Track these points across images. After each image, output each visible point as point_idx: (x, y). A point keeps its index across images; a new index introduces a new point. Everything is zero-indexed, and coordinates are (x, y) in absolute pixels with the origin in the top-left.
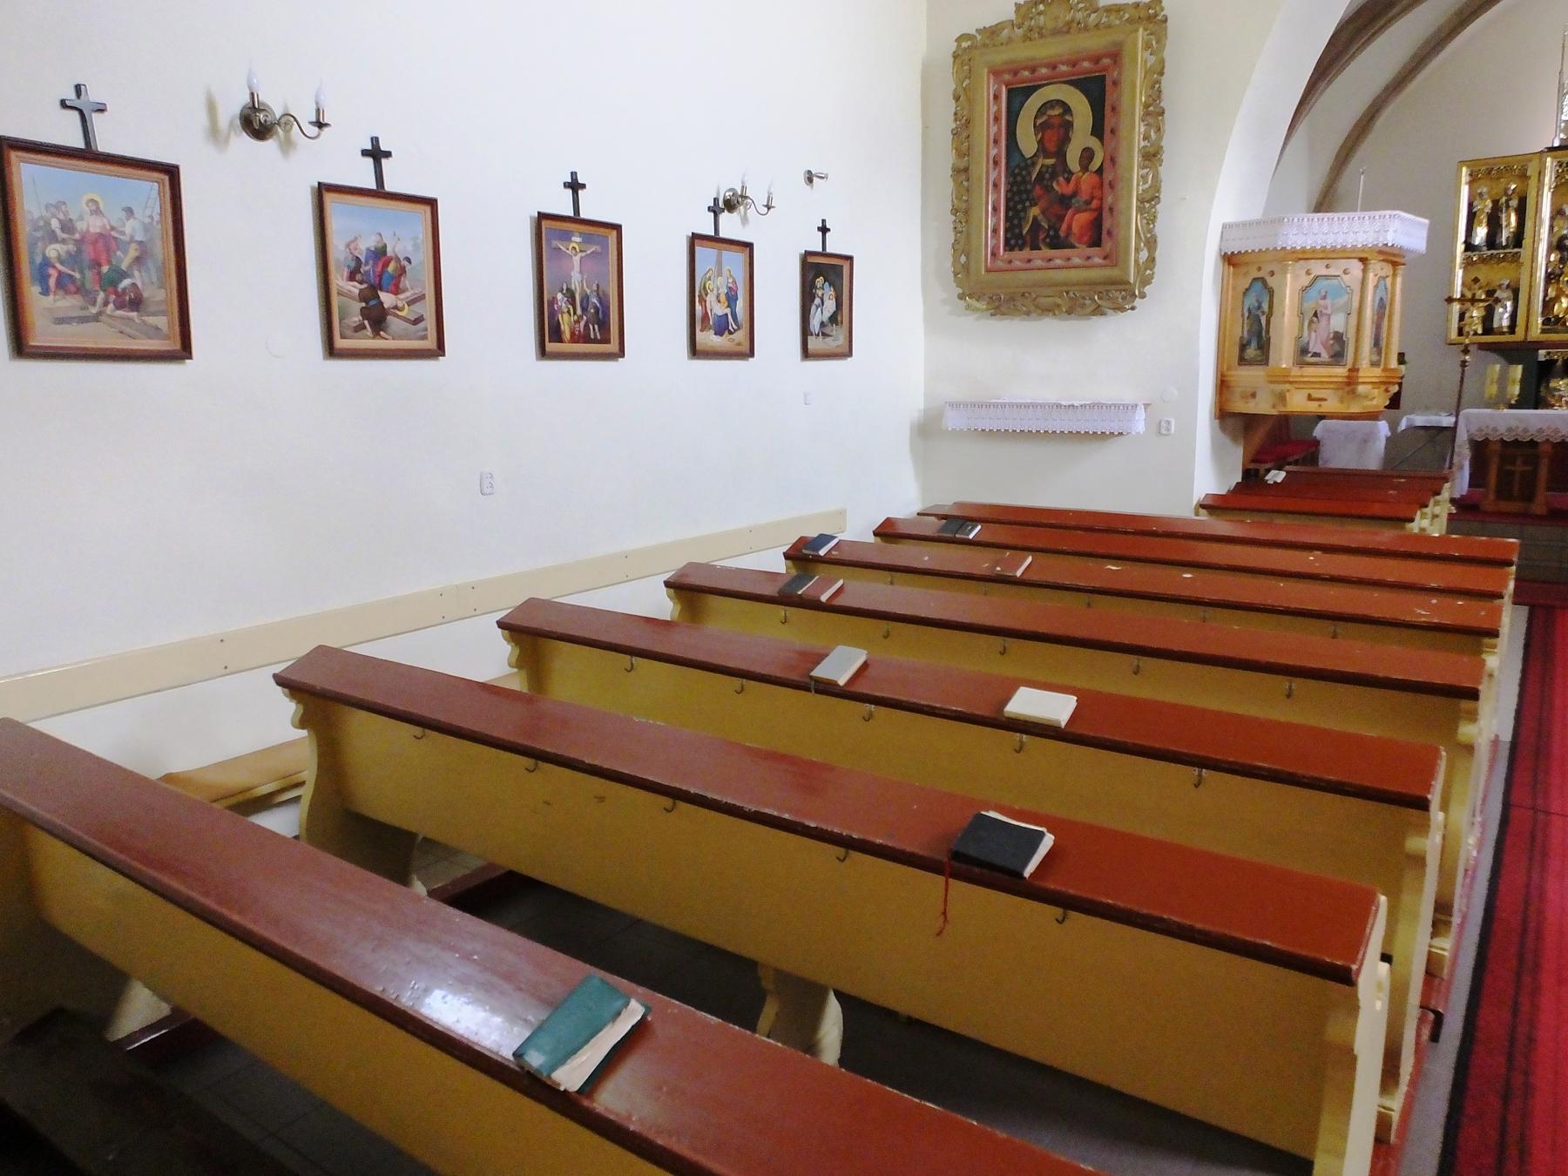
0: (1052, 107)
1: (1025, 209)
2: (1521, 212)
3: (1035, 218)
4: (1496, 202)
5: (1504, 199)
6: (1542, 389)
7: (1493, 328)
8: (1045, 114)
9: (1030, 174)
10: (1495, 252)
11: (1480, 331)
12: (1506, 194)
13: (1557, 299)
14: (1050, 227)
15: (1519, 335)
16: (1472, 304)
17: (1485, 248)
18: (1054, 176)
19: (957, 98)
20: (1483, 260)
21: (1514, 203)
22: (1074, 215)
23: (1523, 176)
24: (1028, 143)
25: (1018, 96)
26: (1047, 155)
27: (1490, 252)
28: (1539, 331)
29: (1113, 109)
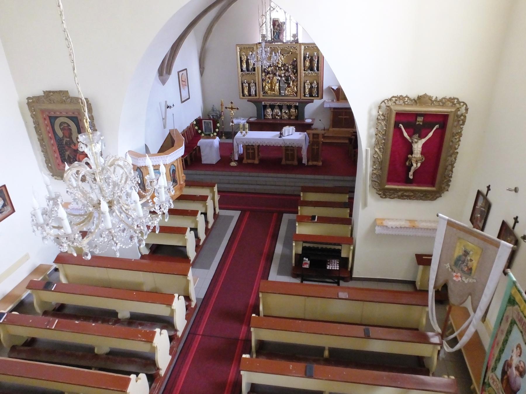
0: (64, 124)
1: (64, 152)
3: (68, 155)
6: (265, 112)
8: (62, 126)
9: (63, 142)
10: (249, 72)
11: (248, 95)
14: (74, 158)
15: (257, 97)
16: (232, 110)
17: (246, 71)
18: (70, 144)
19: (33, 118)
22: (79, 156)
24: (60, 134)
25: (52, 119)
26: (66, 137)
27: (247, 72)
29: (82, 127)
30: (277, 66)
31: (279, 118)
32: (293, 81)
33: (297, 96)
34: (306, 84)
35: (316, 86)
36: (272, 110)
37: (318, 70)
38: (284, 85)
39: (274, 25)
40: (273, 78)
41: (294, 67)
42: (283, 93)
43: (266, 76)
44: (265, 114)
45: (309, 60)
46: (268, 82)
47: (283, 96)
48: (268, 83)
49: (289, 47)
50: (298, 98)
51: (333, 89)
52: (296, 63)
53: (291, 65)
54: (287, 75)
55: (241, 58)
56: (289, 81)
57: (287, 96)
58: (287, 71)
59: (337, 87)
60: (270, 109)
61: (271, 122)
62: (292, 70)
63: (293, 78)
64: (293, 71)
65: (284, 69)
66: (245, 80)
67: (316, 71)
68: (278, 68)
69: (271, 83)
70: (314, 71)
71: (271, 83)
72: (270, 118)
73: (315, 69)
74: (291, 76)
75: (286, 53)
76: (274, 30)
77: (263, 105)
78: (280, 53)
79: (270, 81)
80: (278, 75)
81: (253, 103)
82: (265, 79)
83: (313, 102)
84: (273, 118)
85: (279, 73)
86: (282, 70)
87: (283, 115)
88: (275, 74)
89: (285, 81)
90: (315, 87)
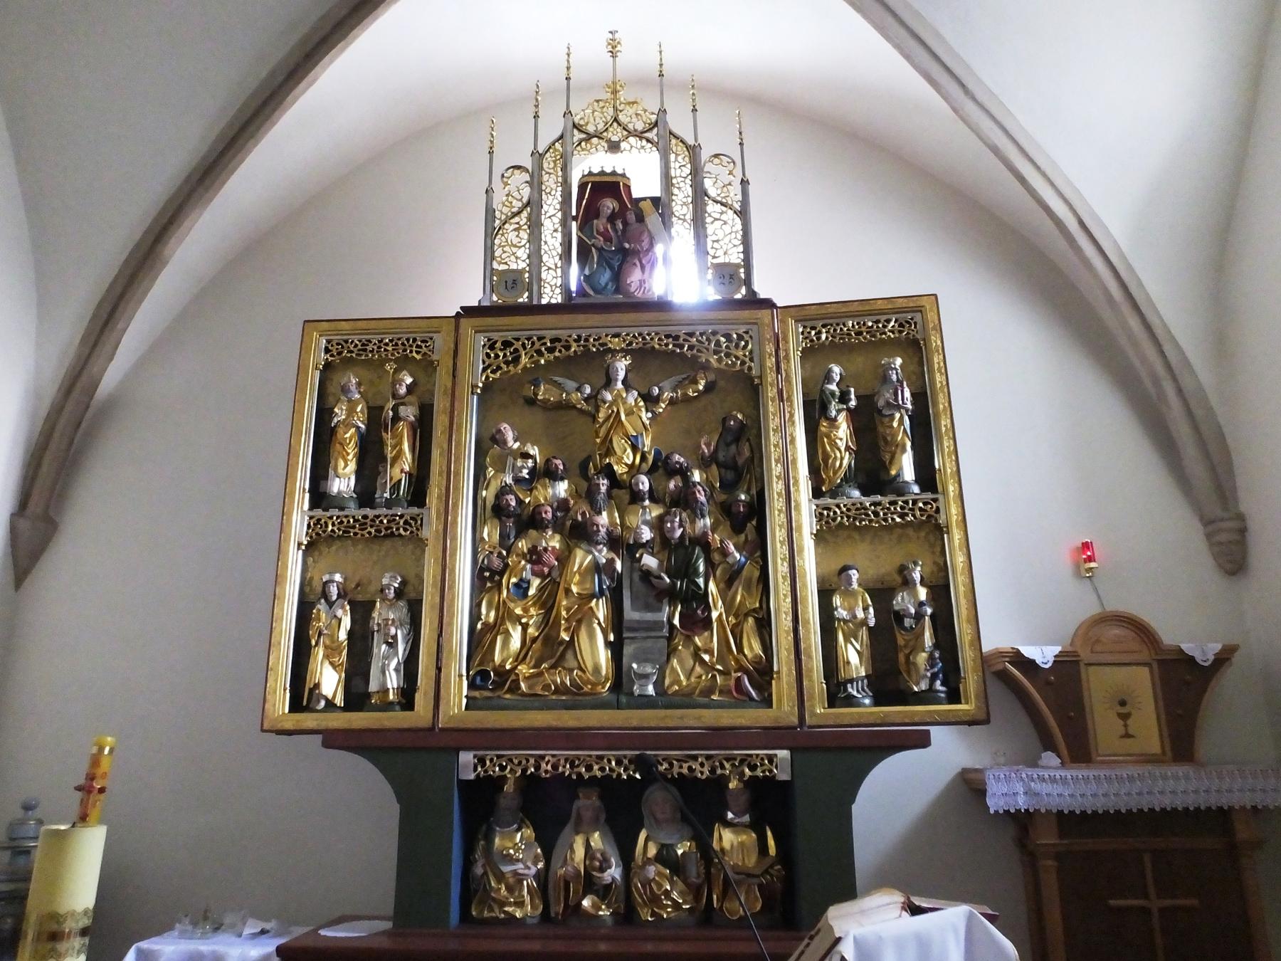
2: (423, 431)
4: (374, 414)
5: (391, 404)
6: (478, 854)
7: (368, 696)
10: (370, 512)
11: (339, 701)
12: (395, 396)
13: (495, 628)
20: (346, 534)
21: (409, 413)
23: (428, 366)
27: (359, 513)
28: (464, 701)
30: (609, 472)
31: (604, 912)
32: (729, 582)
33: (767, 702)
34: (837, 600)
35: (929, 611)
36: (548, 841)
37: (927, 476)
38: (660, 610)
39: (589, 215)
40: (564, 558)
41: (730, 475)
42: (646, 676)
44: (479, 870)
45: (842, 418)
46: (522, 587)
47: (645, 703)
48: (525, 595)
49: (691, 335)
51: (1028, 665)
52: (747, 452)
53: (704, 464)
54: (679, 533)
55: (324, 414)
56: (697, 574)
57: (685, 700)
58: (684, 500)
59: (1057, 649)
60: (529, 832)
61: (536, 946)
62: (723, 497)
63: (724, 553)
64: (726, 511)
65: (654, 497)
66: (331, 573)
67: (916, 489)
68: (604, 484)
69: (547, 602)
70: (901, 494)
72: (518, 914)
73: (906, 467)
74: (716, 539)
75: (666, 384)
76: (591, 237)
77: (464, 785)
79: (536, 582)
80: (609, 533)
81: (376, 763)
82: (497, 563)
83: (922, 741)
84: (546, 917)
85: (612, 523)
86: (636, 497)
87: (647, 883)
88: (580, 533)
89: (668, 580)
90: (919, 617)
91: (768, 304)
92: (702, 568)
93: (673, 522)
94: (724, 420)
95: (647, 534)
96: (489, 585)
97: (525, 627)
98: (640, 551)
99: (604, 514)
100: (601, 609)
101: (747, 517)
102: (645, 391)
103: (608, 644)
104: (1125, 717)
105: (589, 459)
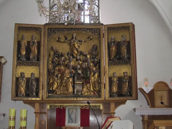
43: (54, 68)
46: (57, 76)
50: (102, 99)
71: (62, 78)
78: (75, 38)
79: (60, 75)
80: (72, 66)
89: (83, 75)
91: (102, 24)
92: (89, 73)
93: (84, 65)
94: (93, 46)
95: (79, 67)
96: (51, 75)
97: (58, 83)
98: (78, 70)
99: (72, 63)
100: (71, 80)
101: (97, 64)
102: (79, 40)
103: (72, 86)
104: (161, 100)
105: (69, 52)
